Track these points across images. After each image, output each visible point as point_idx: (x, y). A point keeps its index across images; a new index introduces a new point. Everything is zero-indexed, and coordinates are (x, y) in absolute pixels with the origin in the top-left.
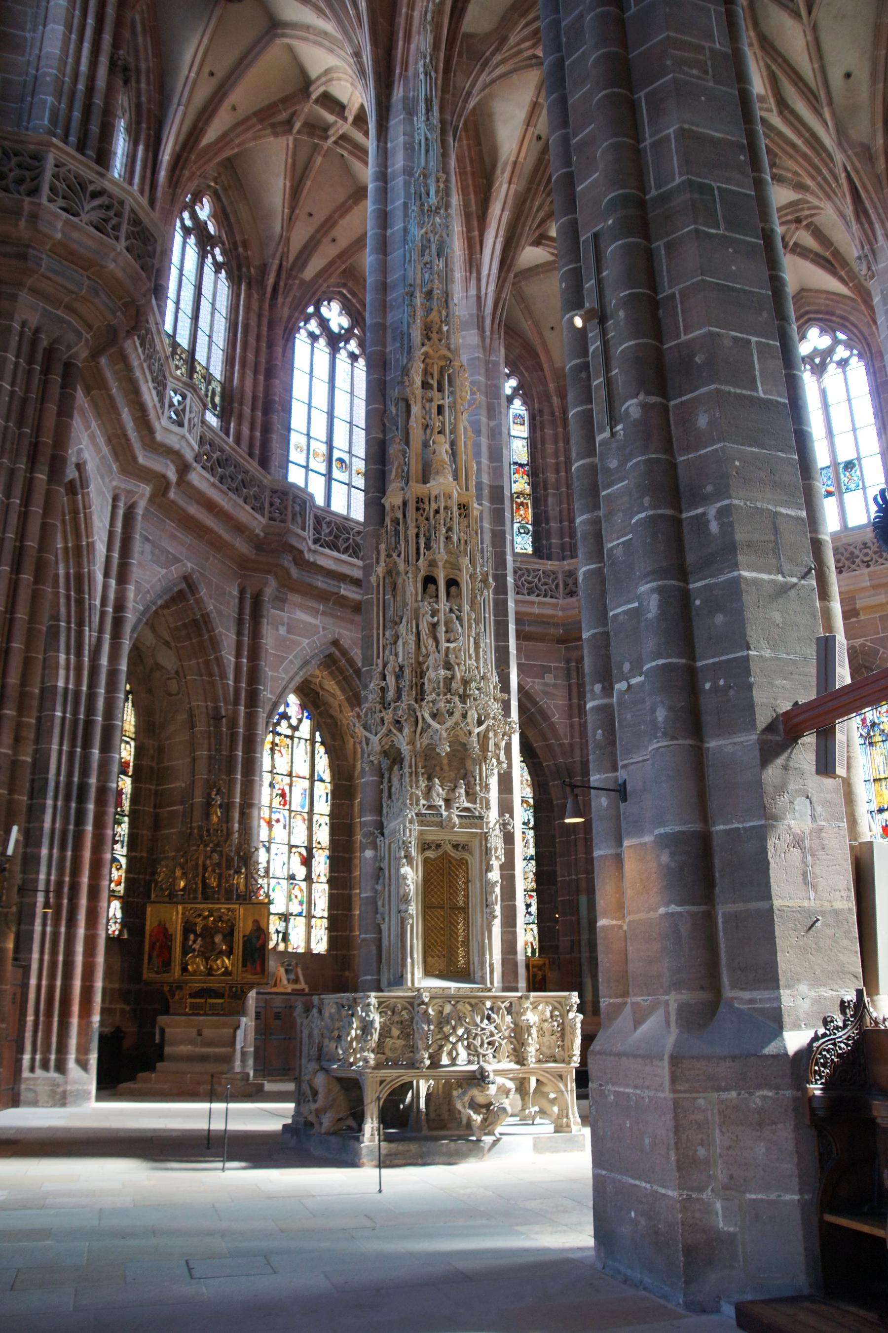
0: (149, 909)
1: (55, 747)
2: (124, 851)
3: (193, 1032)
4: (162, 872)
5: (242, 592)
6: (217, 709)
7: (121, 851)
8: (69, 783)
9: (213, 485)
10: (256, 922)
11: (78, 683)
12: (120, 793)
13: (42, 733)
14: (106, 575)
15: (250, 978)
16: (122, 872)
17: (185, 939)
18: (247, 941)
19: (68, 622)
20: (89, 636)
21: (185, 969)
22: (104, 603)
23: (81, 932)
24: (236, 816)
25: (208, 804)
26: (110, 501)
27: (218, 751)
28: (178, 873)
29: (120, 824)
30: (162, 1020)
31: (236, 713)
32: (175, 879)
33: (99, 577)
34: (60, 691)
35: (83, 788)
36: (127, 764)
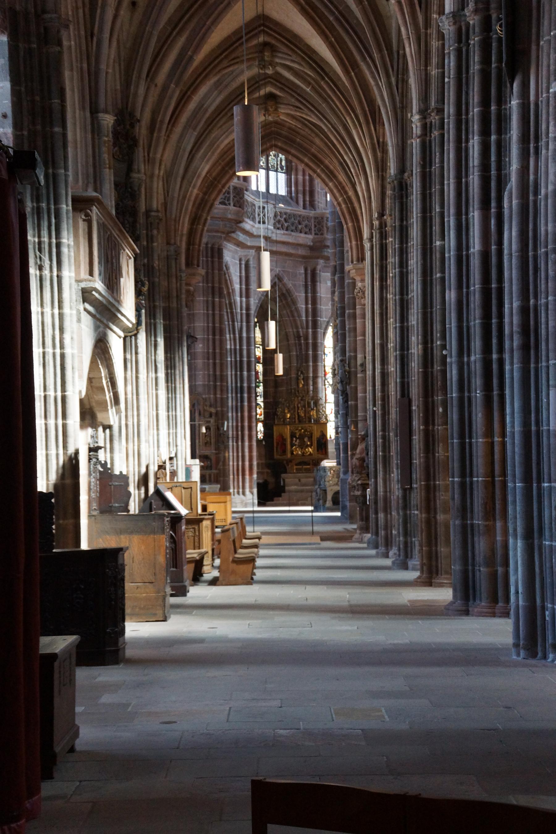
0: (275, 428)
1: (229, 373)
2: (262, 399)
3: (297, 480)
4: (279, 410)
5: (306, 270)
6: (298, 332)
7: (260, 400)
8: (236, 387)
9: (284, 234)
10: (322, 432)
11: (235, 345)
12: (257, 373)
13: (223, 366)
14: (241, 296)
15: (320, 456)
16: (262, 410)
17: (292, 440)
18: (319, 441)
19: (228, 322)
20: (237, 325)
21: (292, 453)
22: (241, 310)
23: (247, 444)
24: (311, 383)
25: (297, 379)
26: (238, 262)
27: (301, 352)
28: (286, 411)
29: (258, 387)
30: (283, 475)
31: (307, 333)
32: (285, 413)
33: (238, 299)
34: (229, 350)
35: (242, 387)
36: (259, 358)
